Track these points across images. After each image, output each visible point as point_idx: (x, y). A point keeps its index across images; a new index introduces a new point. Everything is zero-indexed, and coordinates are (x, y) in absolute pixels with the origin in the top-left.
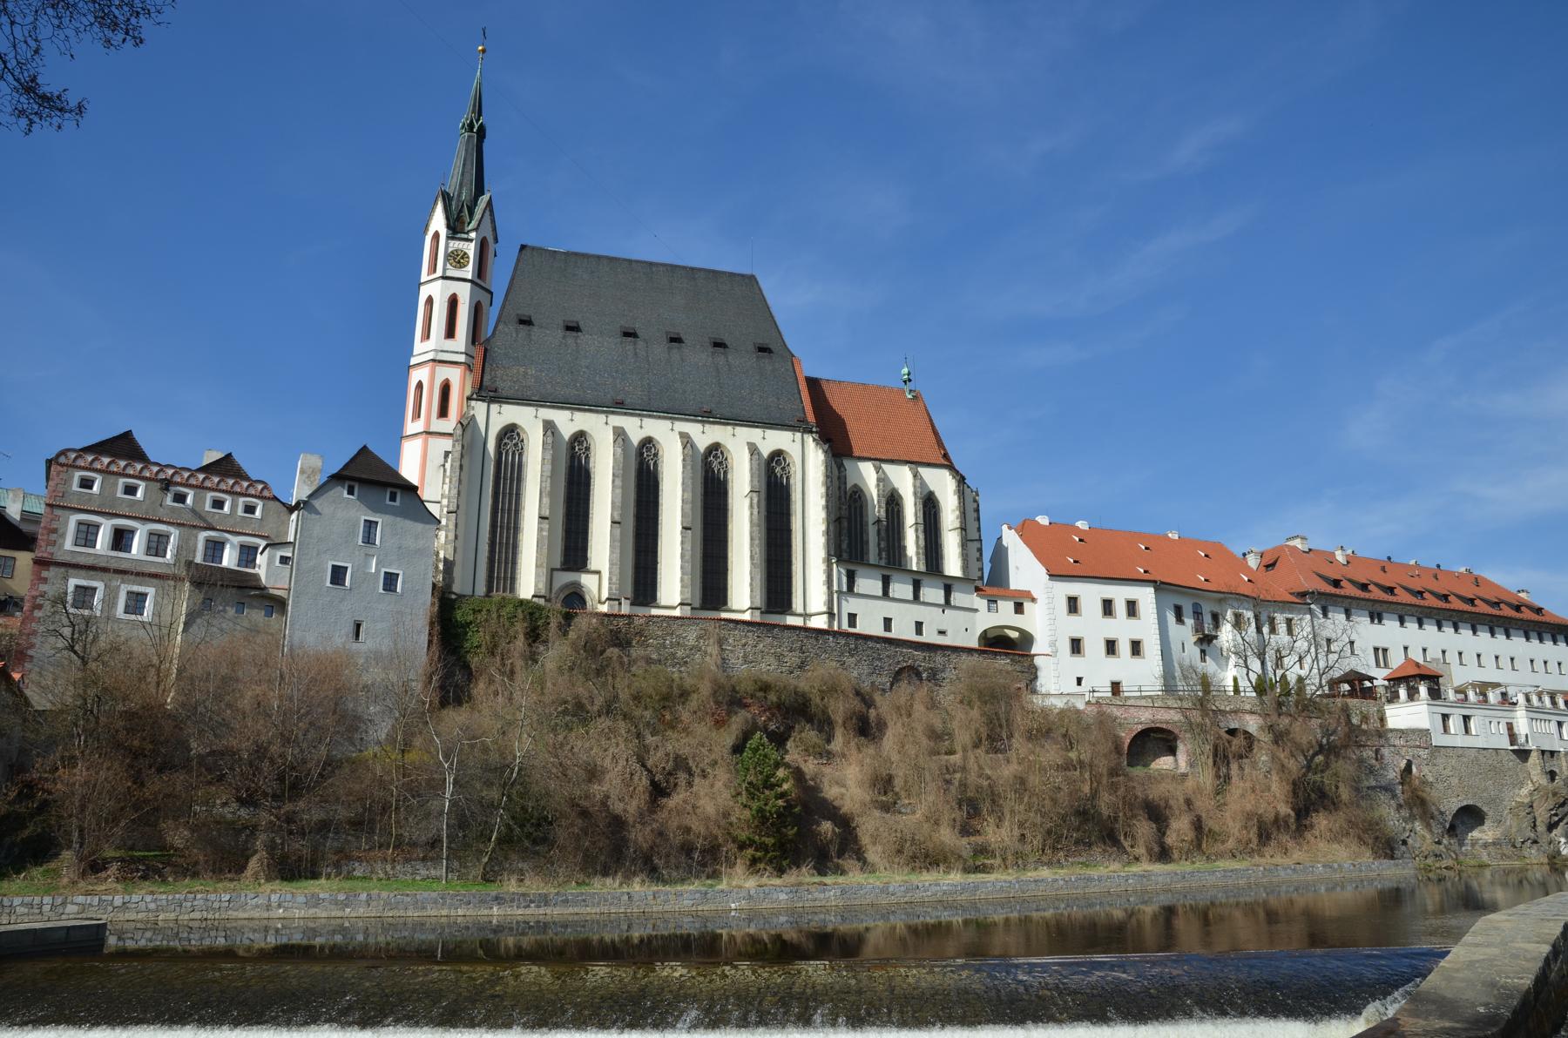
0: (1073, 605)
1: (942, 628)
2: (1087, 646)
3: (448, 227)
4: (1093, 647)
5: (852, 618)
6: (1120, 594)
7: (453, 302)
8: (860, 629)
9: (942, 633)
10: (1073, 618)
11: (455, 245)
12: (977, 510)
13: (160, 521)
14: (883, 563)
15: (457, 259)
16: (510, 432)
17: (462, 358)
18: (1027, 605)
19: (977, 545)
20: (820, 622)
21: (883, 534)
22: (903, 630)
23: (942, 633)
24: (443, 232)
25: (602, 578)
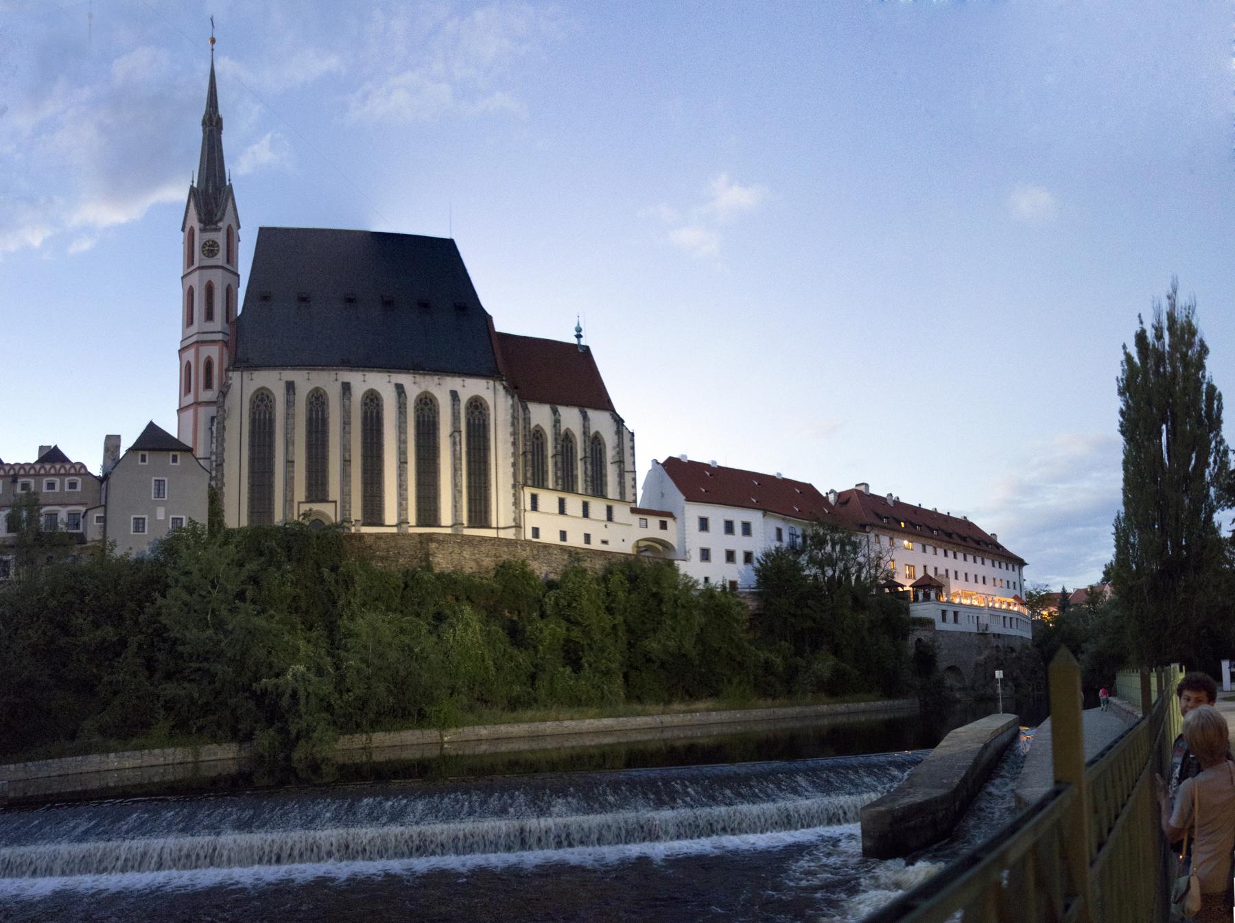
1: (605, 538)
3: (200, 221)
5: (536, 532)
9: (605, 542)
11: (211, 236)
12: (633, 448)
14: (559, 487)
18: (669, 521)
19: (631, 475)
20: (510, 534)
21: (559, 465)
22: (575, 540)
23: (605, 542)
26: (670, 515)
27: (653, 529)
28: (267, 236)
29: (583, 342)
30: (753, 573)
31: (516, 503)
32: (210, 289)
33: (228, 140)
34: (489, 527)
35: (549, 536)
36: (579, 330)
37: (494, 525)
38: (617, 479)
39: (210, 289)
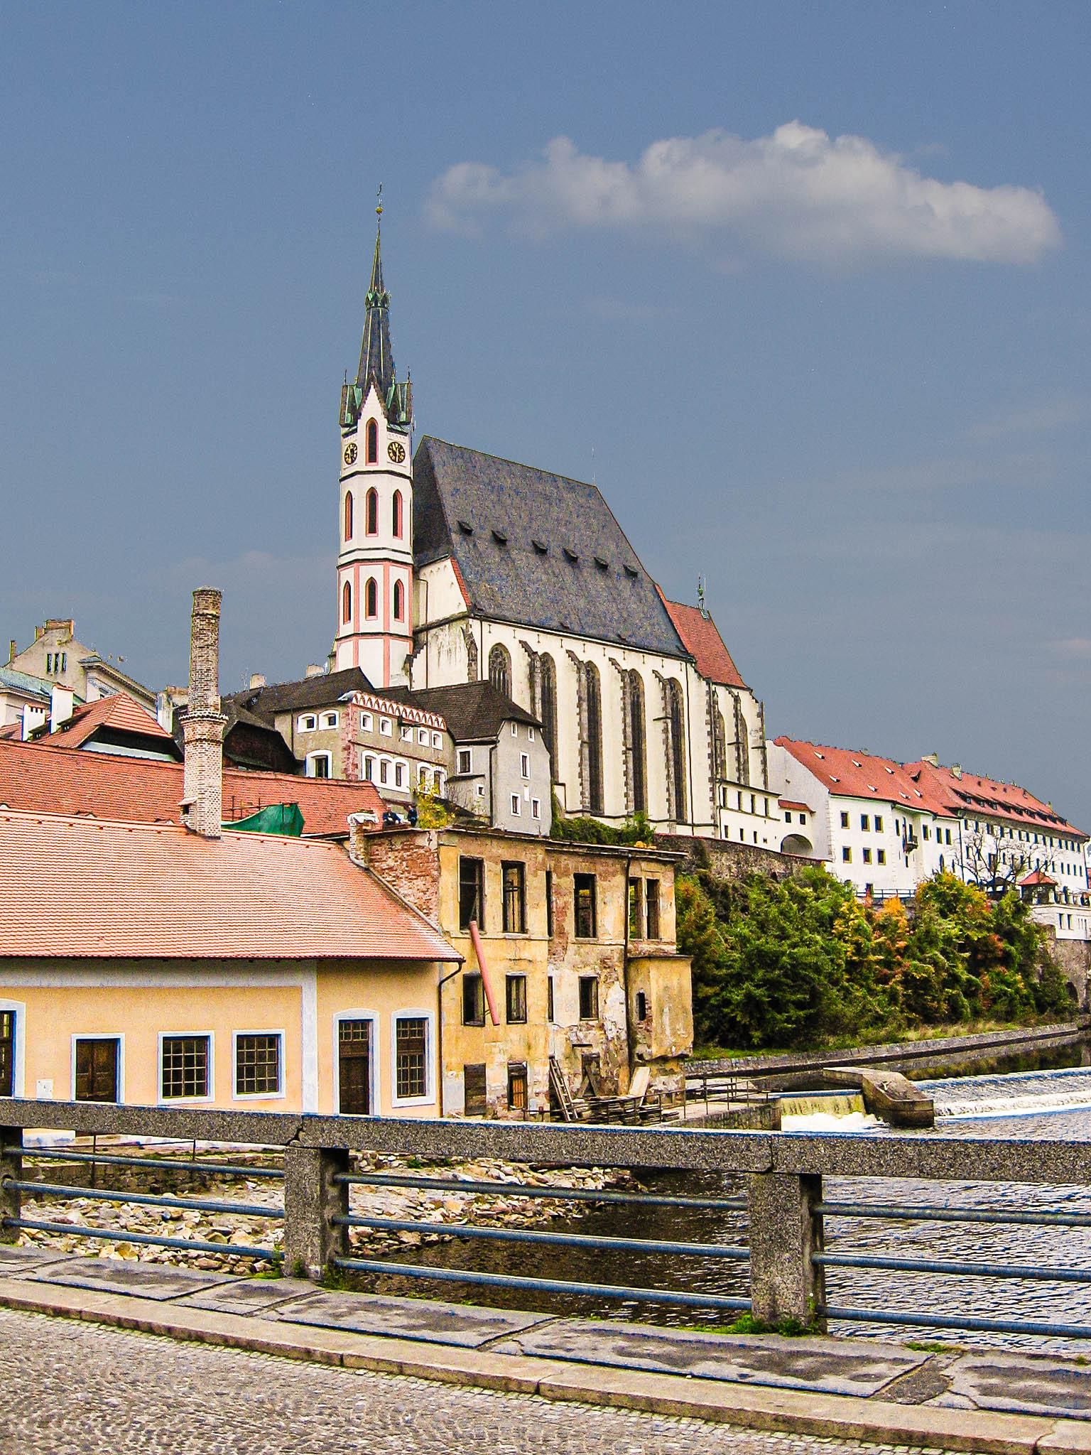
0: (844, 816)
2: (853, 853)
4: (857, 855)
6: (872, 810)
13: (401, 755)
15: (396, 453)
17: (409, 559)
22: (748, 840)
24: (382, 423)
26: (812, 813)
27: (795, 827)
31: (713, 799)
35: (734, 837)
37: (689, 822)
38: (760, 767)
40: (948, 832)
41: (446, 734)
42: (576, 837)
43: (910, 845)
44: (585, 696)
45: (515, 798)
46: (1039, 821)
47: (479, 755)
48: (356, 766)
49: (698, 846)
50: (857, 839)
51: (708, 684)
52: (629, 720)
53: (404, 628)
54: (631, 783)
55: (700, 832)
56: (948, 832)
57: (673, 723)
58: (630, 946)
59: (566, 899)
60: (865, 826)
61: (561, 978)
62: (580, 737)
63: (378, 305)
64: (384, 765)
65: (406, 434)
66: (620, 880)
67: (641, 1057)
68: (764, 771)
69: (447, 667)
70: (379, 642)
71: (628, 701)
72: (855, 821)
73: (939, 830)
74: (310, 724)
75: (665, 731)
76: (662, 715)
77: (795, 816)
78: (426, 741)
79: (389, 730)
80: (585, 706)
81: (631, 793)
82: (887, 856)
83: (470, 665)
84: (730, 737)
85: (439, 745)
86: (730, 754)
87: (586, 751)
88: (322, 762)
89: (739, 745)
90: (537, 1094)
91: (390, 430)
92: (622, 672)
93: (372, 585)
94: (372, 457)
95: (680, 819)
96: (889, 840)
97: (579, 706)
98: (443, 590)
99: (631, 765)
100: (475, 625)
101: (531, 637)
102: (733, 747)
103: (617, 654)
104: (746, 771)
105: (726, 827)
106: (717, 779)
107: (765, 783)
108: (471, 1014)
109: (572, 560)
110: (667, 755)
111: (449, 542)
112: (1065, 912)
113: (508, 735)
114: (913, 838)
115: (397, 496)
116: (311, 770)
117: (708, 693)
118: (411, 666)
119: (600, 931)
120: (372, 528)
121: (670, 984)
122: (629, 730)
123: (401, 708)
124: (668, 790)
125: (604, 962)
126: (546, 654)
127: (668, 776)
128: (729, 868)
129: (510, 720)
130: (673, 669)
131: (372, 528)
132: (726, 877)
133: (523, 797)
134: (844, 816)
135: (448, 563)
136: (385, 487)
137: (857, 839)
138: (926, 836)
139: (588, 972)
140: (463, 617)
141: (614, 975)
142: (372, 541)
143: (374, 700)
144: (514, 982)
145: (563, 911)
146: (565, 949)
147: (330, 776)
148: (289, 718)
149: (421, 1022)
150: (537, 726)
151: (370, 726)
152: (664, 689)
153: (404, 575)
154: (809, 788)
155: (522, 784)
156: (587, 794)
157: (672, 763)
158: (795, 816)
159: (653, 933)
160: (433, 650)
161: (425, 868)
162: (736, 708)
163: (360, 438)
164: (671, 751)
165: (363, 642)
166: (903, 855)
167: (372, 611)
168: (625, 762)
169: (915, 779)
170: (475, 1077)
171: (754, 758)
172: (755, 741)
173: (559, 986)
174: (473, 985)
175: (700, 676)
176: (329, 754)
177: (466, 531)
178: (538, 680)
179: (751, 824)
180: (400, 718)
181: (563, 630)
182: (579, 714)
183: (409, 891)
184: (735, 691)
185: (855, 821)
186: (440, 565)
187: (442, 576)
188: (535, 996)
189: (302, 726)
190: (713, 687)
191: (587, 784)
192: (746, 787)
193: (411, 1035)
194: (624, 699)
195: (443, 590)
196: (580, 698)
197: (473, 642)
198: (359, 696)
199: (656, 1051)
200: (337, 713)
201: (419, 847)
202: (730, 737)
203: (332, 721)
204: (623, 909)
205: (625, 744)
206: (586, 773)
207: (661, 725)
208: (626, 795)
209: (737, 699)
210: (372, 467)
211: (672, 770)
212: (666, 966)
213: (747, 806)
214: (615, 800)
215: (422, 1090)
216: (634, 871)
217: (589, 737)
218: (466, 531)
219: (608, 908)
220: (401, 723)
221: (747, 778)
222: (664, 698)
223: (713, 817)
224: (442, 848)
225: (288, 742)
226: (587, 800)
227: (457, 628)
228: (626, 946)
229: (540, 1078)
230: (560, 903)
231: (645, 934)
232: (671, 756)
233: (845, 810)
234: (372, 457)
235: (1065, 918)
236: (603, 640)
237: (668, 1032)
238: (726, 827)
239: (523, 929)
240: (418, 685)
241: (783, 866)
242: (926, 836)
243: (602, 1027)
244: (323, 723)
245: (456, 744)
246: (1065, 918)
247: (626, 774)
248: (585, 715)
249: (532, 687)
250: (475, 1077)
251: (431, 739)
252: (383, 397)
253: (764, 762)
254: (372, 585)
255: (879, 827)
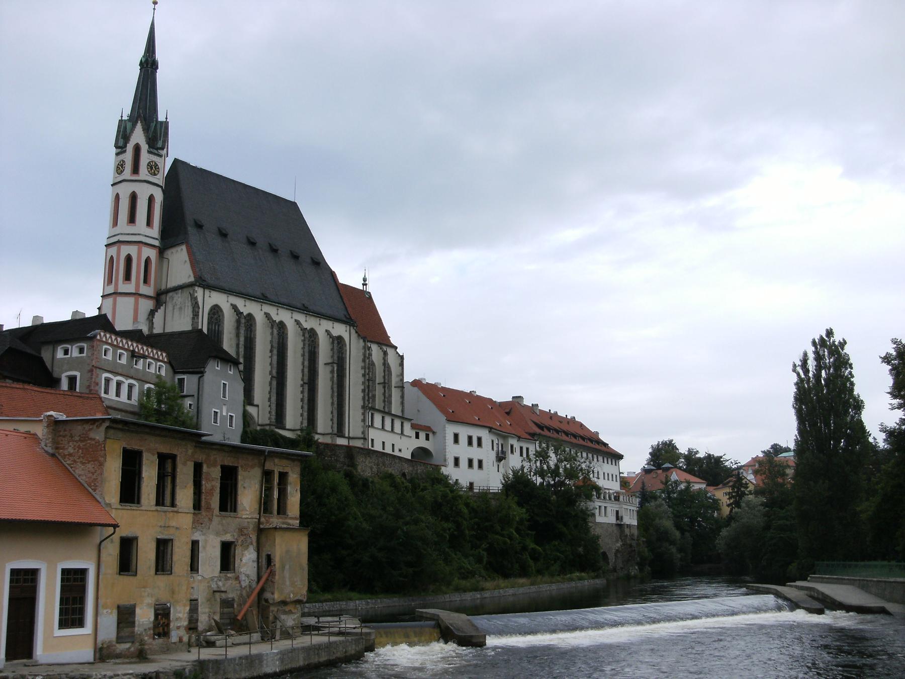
0: (456, 436)
4: (464, 463)
6: (476, 433)
7: (151, 199)
8: (375, 448)
10: (456, 446)
13: (132, 378)
16: (216, 311)
17: (157, 243)
20: (358, 444)
22: (388, 450)
24: (144, 147)
25: (293, 418)
26: (434, 433)
27: (422, 442)
28: (176, 162)
29: (369, 289)
30: (501, 486)
31: (364, 420)
32: (134, 197)
33: (161, 76)
34: (344, 437)
35: (378, 447)
36: (365, 280)
37: (347, 435)
38: (400, 400)
39: (134, 197)
40: (527, 449)
41: (168, 366)
42: (259, 441)
43: (501, 457)
44: (275, 345)
45: (216, 413)
46: (590, 444)
47: (190, 382)
48: (97, 384)
49: (350, 452)
50: (463, 451)
51: (364, 341)
52: (306, 363)
53: (149, 290)
54: (306, 407)
55: (354, 443)
56: (527, 449)
57: (338, 367)
58: (263, 519)
59: (214, 483)
60: (470, 443)
61: (206, 541)
62: (271, 373)
63: (149, 65)
64: (119, 384)
65: (161, 156)
66: (257, 473)
67: (266, 601)
68: (402, 403)
69: (177, 320)
70: (131, 300)
71: (307, 349)
72: (463, 440)
73: (521, 448)
74: (66, 352)
75: (332, 372)
76: (330, 361)
77: (422, 435)
78: (152, 370)
79: (124, 361)
80: (275, 352)
81: (305, 414)
82: (484, 464)
83: (193, 318)
84: (379, 378)
85: (163, 373)
86: (379, 390)
87: (274, 383)
88: (72, 380)
89: (386, 384)
90: (178, 628)
91: (149, 152)
92: (304, 330)
93: (129, 259)
94: (136, 169)
95: (340, 433)
96: (487, 454)
97: (271, 351)
98: (179, 267)
99: (306, 395)
100: (199, 292)
101: (240, 303)
102: (381, 386)
103: (301, 318)
104: (390, 403)
105: (372, 440)
106: (368, 407)
107: (403, 411)
108: (126, 565)
109: (274, 250)
110: (332, 388)
111: (186, 233)
112: (603, 505)
113: (214, 369)
114: (503, 452)
115: (151, 199)
116: (65, 385)
117: (364, 348)
118: (153, 317)
119: (239, 507)
120: (132, 219)
121: (292, 549)
122: (306, 370)
123: (135, 345)
124: (332, 413)
125: (241, 531)
126: (250, 315)
127: (332, 404)
128: (371, 468)
129: (215, 357)
130: (340, 330)
131: (132, 219)
132: (368, 474)
133: (221, 412)
134: (456, 436)
135: (184, 247)
136: (144, 193)
137: (463, 451)
138: (512, 452)
139: (228, 538)
140: (191, 285)
141: (249, 541)
142: (131, 229)
143: (113, 337)
144: (163, 546)
145: (211, 492)
146: (211, 520)
147: (78, 390)
148: (51, 348)
149: (83, 572)
150: (235, 362)
151: (110, 357)
152: (333, 343)
153: (152, 254)
154: (432, 415)
155: (220, 405)
156: (274, 413)
157: (336, 394)
158: (422, 435)
159: (282, 510)
160: (170, 307)
161: (95, 455)
162: (384, 359)
163: (128, 156)
164: (335, 386)
165: (120, 299)
166: (496, 464)
167: (128, 277)
168: (302, 392)
169: (508, 413)
170: (126, 616)
171: (395, 394)
172: (397, 383)
173: (204, 548)
174: (128, 546)
175: (359, 335)
176: (78, 374)
177: (199, 226)
178: (242, 331)
179: (390, 439)
180: (133, 352)
181: (263, 299)
182: (271, 357)
183: (81, 471)
184: (385, 348)
185: (463, 440)
186: (179, 248)
187: (179, 257)
188: (180, 555)
189: (60, 354)
190: (369, 344)
191: (274, 406)
192: (389, 414)
193: (74, 582)
194: (303, 348)
195: (179, 267)
196: (272, 346)
197: (197, 303)
198: (102, 334)
199: (277, 597)
200: (85, 345)
201: (91, 439)
202: (379, 378)
203: (81, 350)
204: (258, 493)
205: (302, 380)
206: (274, 399)
207: (329, 368)
208: (302, 415)
209: (385, 353)
210: (135, 177)
211: (335, 399)
212: (288, 535)
213: (388, 426)
214: (293, 418)
215: (80, 623)
216: (269, 466)
217: (277, 373)
218: (199, 226)
219: (246, 492)
220: (133, 355)
221: (390, 407)
222: (332, 349)
223: (363, 433)
224: (108, 440)
225: (49, 367)
226: (273, 417)
227: (186, 293)
228: (259, 519)
229: (181, 615)
230: (209, 486)
231: (275, 512)
232: (335, 389)
233: (456, 431)
234: (136, 169)
235: (603, 508)
236: (291, 307)
237: (288, 583)
238: (372, 440)
239: (173, 505)
240: (158, 330)
241: (411, 469)
242: (512, 452)
243: (237, 578)
244: (75, 353)
245: (175, 372)
246: (603, 508)
247: (302, 400)
248: (275, 358)
249: (238, 335)
250: (126, 616)
251: (156, 366)
252: (146, 130)
253: (402, 397)
254: (129, 259)
255: (480, 444)
